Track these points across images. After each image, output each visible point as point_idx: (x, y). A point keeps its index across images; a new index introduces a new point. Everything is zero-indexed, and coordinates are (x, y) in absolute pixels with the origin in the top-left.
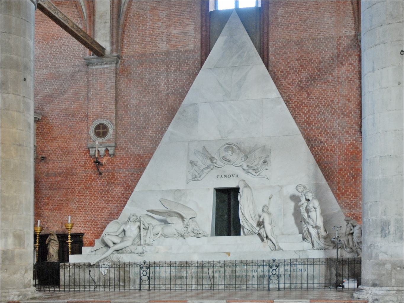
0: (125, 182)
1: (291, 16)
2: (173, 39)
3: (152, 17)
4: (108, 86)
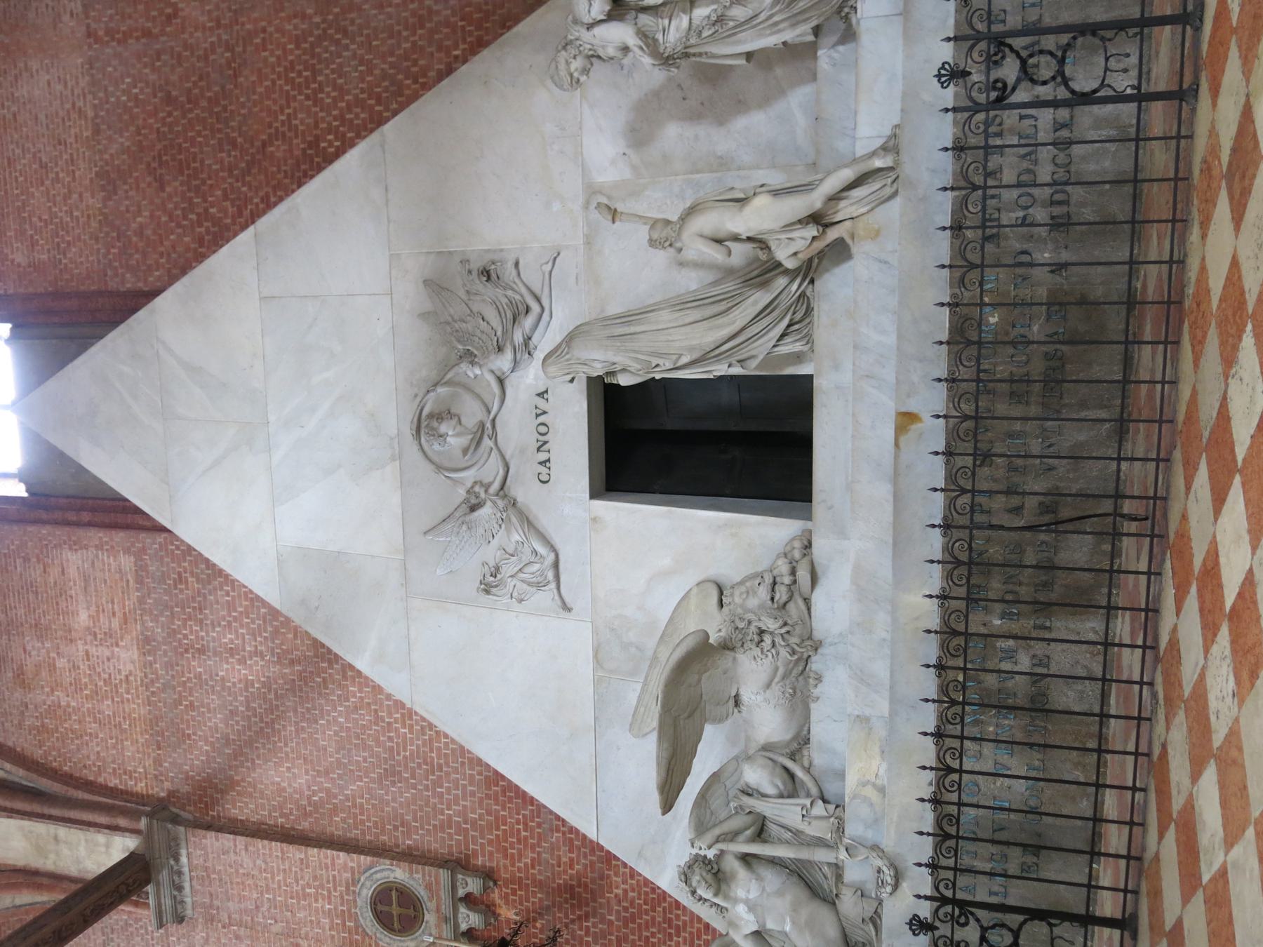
1: (30, 216)
3: (43, 687)
4: (247, 862)
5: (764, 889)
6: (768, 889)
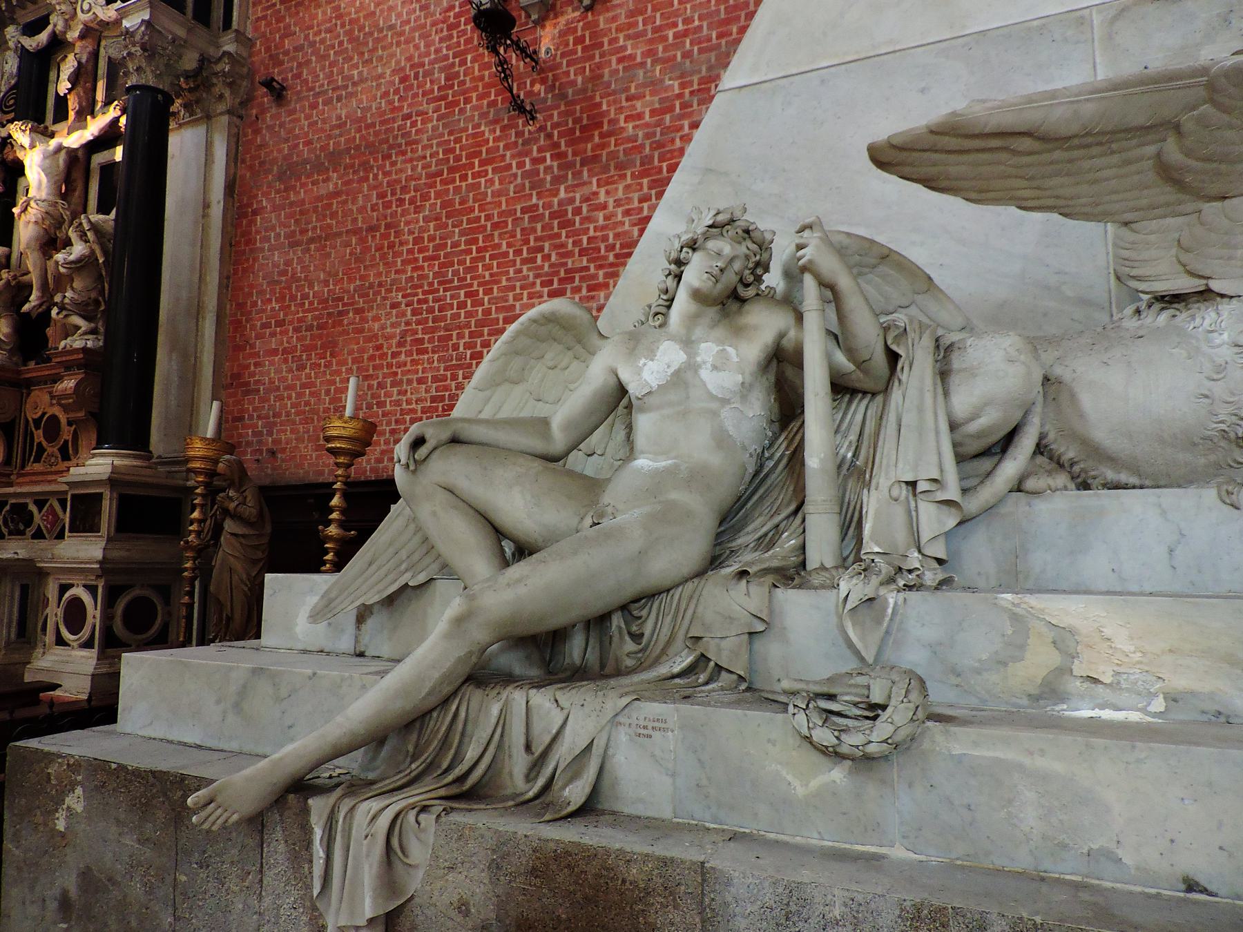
0: (659, 145)
5: (725, 402)
6: (725, 413)
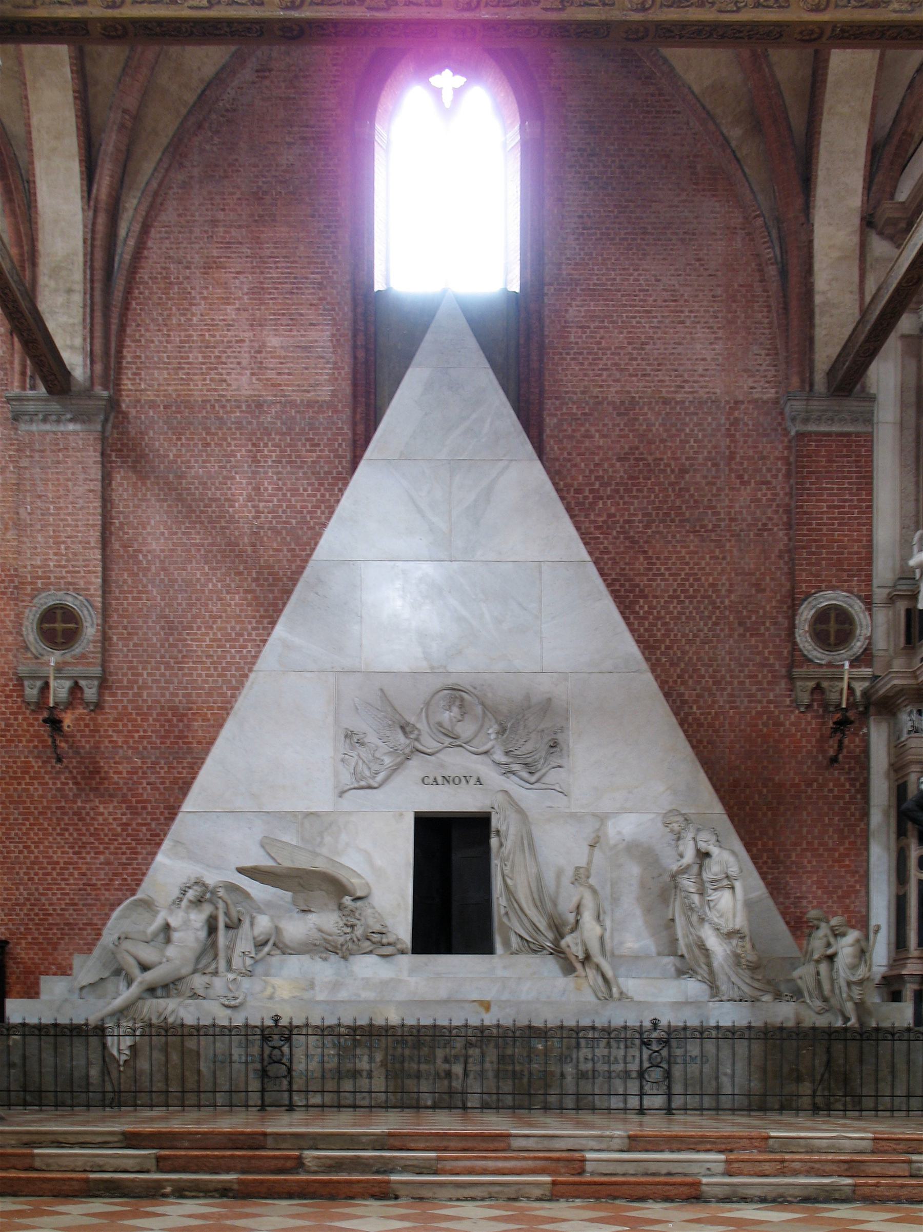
0: (130, 789)
2: (271, 363)
3: (207, 288)
4: (81, 490)
